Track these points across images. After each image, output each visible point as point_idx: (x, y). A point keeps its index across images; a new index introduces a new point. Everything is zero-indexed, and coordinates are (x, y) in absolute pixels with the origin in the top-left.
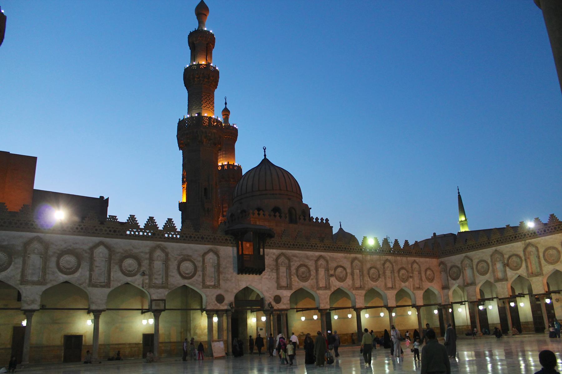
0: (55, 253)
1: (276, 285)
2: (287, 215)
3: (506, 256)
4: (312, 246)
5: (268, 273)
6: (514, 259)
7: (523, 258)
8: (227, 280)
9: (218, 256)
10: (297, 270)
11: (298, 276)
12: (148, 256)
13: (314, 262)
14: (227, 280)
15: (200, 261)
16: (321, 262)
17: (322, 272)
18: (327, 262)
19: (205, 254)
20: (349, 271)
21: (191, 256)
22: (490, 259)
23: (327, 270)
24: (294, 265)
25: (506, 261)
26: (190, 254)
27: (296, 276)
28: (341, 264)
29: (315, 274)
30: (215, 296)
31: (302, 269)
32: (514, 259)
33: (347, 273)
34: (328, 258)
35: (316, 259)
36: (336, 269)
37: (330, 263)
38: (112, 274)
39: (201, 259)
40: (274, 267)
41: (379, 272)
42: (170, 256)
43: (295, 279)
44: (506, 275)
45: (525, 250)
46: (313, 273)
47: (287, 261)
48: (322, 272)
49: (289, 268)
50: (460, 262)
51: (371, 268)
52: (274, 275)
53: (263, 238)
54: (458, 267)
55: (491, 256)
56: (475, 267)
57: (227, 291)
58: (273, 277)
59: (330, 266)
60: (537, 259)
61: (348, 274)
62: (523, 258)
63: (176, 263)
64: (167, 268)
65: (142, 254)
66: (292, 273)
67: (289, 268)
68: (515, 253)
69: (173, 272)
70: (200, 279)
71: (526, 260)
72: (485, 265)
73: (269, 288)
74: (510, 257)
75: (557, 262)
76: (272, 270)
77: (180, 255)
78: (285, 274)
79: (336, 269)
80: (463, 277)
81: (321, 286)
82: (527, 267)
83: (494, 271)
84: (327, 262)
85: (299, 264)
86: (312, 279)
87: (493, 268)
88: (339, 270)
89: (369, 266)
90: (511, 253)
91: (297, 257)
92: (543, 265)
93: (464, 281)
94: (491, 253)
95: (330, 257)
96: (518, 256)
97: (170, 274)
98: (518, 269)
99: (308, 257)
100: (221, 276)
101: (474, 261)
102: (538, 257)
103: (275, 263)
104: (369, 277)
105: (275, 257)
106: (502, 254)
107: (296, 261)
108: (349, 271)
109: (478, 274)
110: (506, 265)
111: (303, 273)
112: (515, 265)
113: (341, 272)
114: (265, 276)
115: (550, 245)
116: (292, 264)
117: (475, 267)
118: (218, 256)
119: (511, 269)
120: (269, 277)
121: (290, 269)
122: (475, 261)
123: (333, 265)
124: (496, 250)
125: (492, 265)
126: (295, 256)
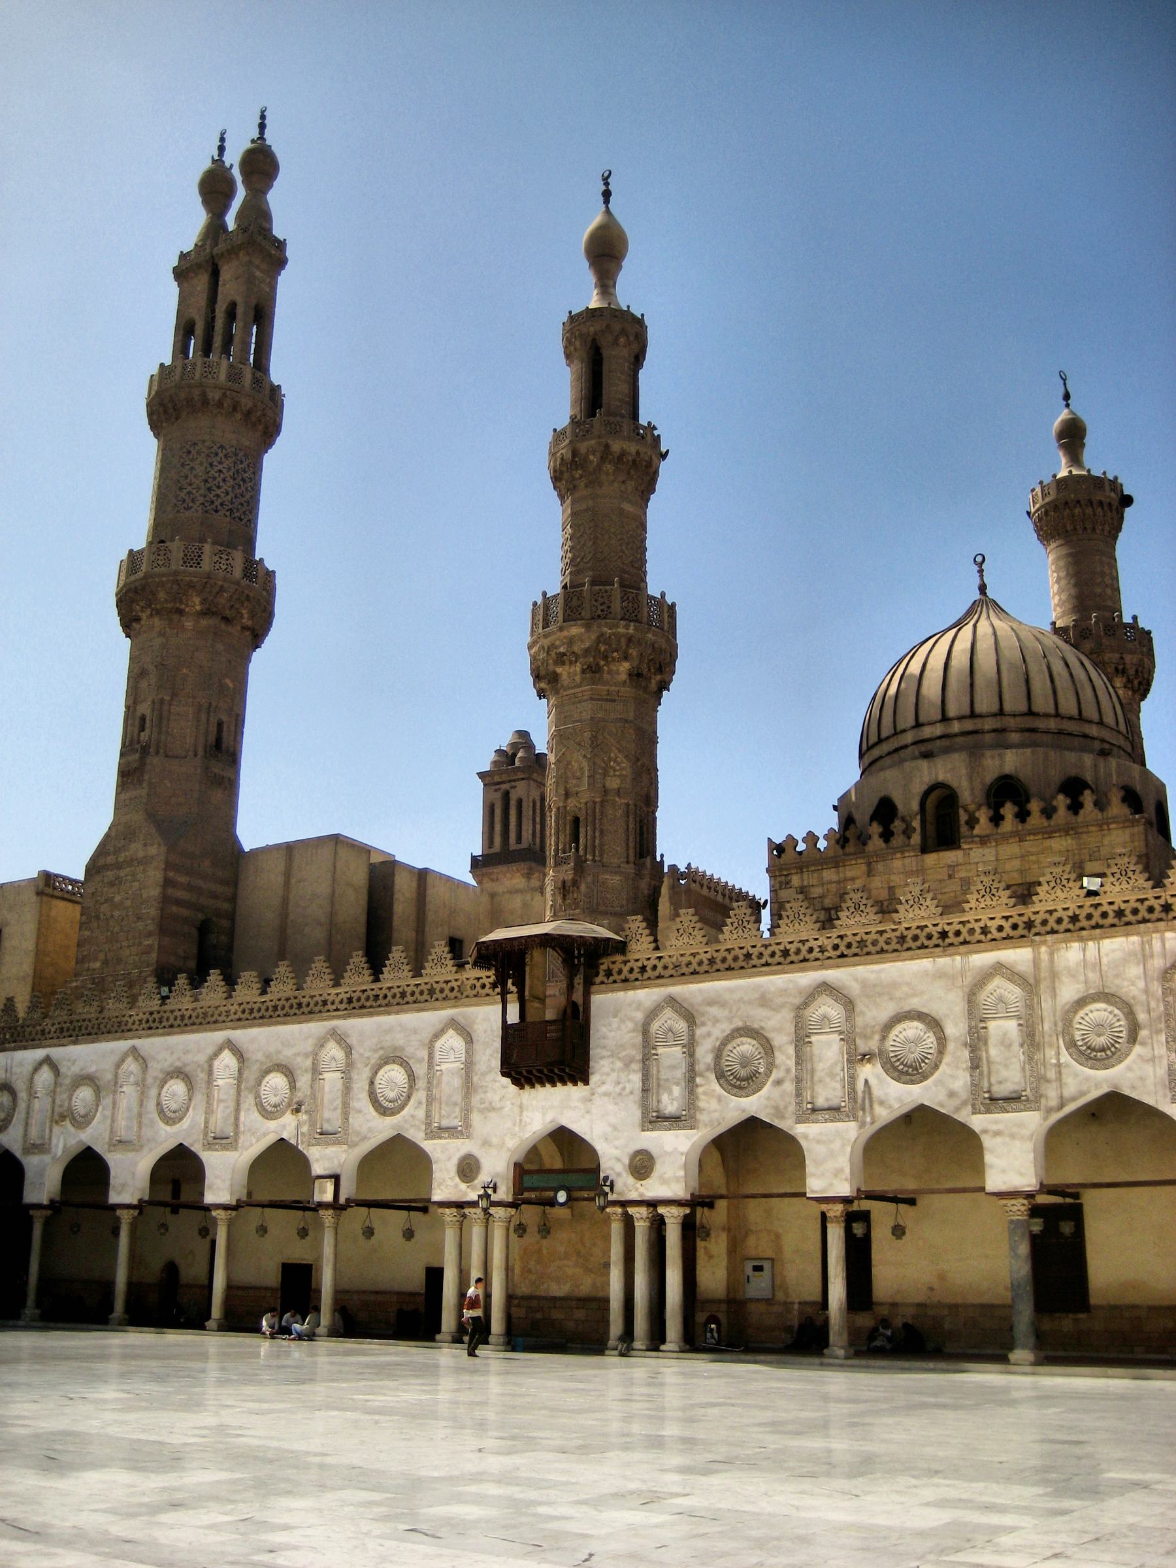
0: (156, 1078)
1: (638, 1114)
2: (916, 824)
4: (786, 953)
5: (614, 1075)
8: (492, 1109)
9: (469, 1039)
10: (718, 1054)
11: (720, 1076)
12: (308, 1063)
13: (792, 1015)
14: (492, 1109)
15: (421, 1061)
16: (824, 1009)
17: (828, 1050)
18: (849, 1004)
19: (437, 1036)
20: (955, 1029)
21: (402, 1049)
23: (848, 1038)
24: (709, 1034)
26: (401, 1042)
27: (713, 1077)
28: (915, 1003)
29: (791, 1063)
30: (455, 1161)
31: (747, 1046)
33: (942, 1041)
34: (854, 989)
35: (797, 1001)
36: (888, 1027)
37: (860, 1006)
38: (242, 1115)
39: (425, 1054)
40: (634, 1052)
41: (1130, 1014)
42: (355, 1055)
43: (709, 1086)
46: (786, 1057)
47: (681, 1026)
48: (828, 1050)
49: (690, 1049)
51: (1081, 1003)
52: (636, 1079)
53: (587, 962)
57: (486, 1143)
58: (629, 1087)
59: (859, 1021)
61: (951, 1047)
63: (366, 1073)
64: (347, 1089)
65: (299, 1059)
66: (700, 1067)
67: (690, 1049)
69: (361, 1101)
70: (421, 1113)
73: (615, 1128)
76: (627, 1066)
77: (376, 1051)
78: (680, 1073)
79: (888, 1027)
81: (821, 1102)
84: (849, 1004)
85: (725, 1028)
86: (778, 1082)
88: (912, 1029)
89: (1069, 992)
91: (722, 1004)
95: (864, 984)
97: (355, 1104)
99: (764, 1001)
100: (475, 1100)
103: (640, 1038)
104: (1071, 1045)
105: (640, 1016)
107: (716, 1021)
108: (955, 1029)
111: (745, 1061)
113: (917, 1041)
114: (604, 1088)
116: (699, 1032)
118: (469, 1039)
120: (618, 1089)
121: (691, 1054)
123: (874, 1014)
126: (711, 1003)
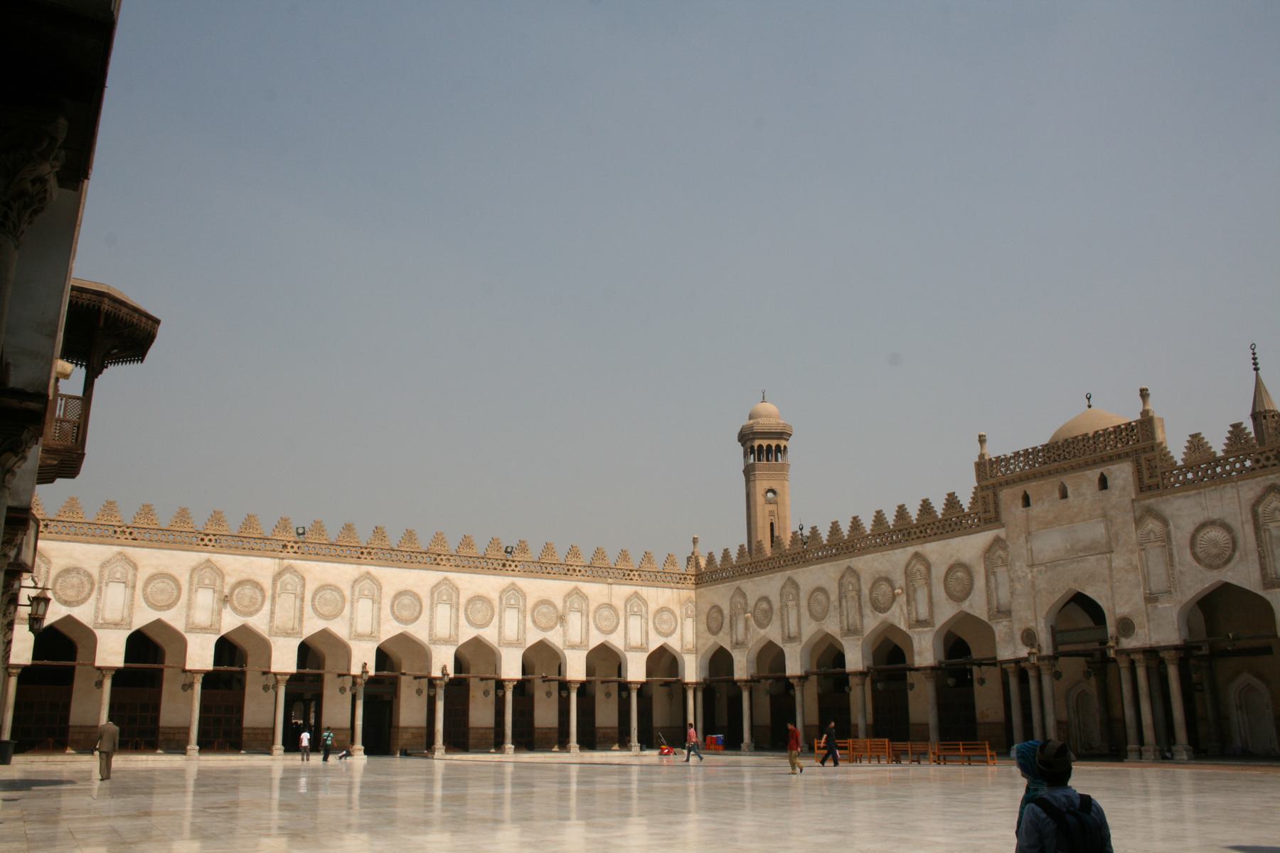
3: (230, 580)
6: (248, 590)
7: (269, 593)
22: (187, 577)
25: (227, 591)
32: (248, 590)
44: (219, 621)
45: (279, 575)
50: (98, 564)
54: (90, 576)
55: (193, 570)
56: (140, 585)
60: (298, 602)
62: (269, 593)
68: (252, 577)
71: (273, 598)
72: (168, 586)
74: (240, 583)
75: (335, 616)
80: (98, 600)
82: (272, 613)
83: (189, 606)
87: (190, 599)
90: (244, 576)
92: (306, 616)
93: (97, 608)
94: (194, 564)
96: (256, 585)
98: (251, 614)
101: (140, 570)
102: (302, 599)
106: (220, 573)
109: (144, 604)
110: (226, 600)
112: (246, 602)
115: (331, 580)
117: (140, 585)
119: (234, 609)
122: (143, 575)
124: (208, 561)
125: (190, 590)
